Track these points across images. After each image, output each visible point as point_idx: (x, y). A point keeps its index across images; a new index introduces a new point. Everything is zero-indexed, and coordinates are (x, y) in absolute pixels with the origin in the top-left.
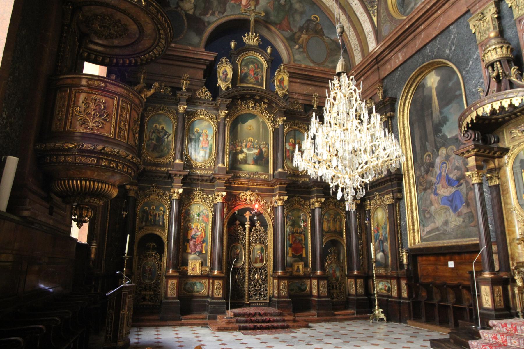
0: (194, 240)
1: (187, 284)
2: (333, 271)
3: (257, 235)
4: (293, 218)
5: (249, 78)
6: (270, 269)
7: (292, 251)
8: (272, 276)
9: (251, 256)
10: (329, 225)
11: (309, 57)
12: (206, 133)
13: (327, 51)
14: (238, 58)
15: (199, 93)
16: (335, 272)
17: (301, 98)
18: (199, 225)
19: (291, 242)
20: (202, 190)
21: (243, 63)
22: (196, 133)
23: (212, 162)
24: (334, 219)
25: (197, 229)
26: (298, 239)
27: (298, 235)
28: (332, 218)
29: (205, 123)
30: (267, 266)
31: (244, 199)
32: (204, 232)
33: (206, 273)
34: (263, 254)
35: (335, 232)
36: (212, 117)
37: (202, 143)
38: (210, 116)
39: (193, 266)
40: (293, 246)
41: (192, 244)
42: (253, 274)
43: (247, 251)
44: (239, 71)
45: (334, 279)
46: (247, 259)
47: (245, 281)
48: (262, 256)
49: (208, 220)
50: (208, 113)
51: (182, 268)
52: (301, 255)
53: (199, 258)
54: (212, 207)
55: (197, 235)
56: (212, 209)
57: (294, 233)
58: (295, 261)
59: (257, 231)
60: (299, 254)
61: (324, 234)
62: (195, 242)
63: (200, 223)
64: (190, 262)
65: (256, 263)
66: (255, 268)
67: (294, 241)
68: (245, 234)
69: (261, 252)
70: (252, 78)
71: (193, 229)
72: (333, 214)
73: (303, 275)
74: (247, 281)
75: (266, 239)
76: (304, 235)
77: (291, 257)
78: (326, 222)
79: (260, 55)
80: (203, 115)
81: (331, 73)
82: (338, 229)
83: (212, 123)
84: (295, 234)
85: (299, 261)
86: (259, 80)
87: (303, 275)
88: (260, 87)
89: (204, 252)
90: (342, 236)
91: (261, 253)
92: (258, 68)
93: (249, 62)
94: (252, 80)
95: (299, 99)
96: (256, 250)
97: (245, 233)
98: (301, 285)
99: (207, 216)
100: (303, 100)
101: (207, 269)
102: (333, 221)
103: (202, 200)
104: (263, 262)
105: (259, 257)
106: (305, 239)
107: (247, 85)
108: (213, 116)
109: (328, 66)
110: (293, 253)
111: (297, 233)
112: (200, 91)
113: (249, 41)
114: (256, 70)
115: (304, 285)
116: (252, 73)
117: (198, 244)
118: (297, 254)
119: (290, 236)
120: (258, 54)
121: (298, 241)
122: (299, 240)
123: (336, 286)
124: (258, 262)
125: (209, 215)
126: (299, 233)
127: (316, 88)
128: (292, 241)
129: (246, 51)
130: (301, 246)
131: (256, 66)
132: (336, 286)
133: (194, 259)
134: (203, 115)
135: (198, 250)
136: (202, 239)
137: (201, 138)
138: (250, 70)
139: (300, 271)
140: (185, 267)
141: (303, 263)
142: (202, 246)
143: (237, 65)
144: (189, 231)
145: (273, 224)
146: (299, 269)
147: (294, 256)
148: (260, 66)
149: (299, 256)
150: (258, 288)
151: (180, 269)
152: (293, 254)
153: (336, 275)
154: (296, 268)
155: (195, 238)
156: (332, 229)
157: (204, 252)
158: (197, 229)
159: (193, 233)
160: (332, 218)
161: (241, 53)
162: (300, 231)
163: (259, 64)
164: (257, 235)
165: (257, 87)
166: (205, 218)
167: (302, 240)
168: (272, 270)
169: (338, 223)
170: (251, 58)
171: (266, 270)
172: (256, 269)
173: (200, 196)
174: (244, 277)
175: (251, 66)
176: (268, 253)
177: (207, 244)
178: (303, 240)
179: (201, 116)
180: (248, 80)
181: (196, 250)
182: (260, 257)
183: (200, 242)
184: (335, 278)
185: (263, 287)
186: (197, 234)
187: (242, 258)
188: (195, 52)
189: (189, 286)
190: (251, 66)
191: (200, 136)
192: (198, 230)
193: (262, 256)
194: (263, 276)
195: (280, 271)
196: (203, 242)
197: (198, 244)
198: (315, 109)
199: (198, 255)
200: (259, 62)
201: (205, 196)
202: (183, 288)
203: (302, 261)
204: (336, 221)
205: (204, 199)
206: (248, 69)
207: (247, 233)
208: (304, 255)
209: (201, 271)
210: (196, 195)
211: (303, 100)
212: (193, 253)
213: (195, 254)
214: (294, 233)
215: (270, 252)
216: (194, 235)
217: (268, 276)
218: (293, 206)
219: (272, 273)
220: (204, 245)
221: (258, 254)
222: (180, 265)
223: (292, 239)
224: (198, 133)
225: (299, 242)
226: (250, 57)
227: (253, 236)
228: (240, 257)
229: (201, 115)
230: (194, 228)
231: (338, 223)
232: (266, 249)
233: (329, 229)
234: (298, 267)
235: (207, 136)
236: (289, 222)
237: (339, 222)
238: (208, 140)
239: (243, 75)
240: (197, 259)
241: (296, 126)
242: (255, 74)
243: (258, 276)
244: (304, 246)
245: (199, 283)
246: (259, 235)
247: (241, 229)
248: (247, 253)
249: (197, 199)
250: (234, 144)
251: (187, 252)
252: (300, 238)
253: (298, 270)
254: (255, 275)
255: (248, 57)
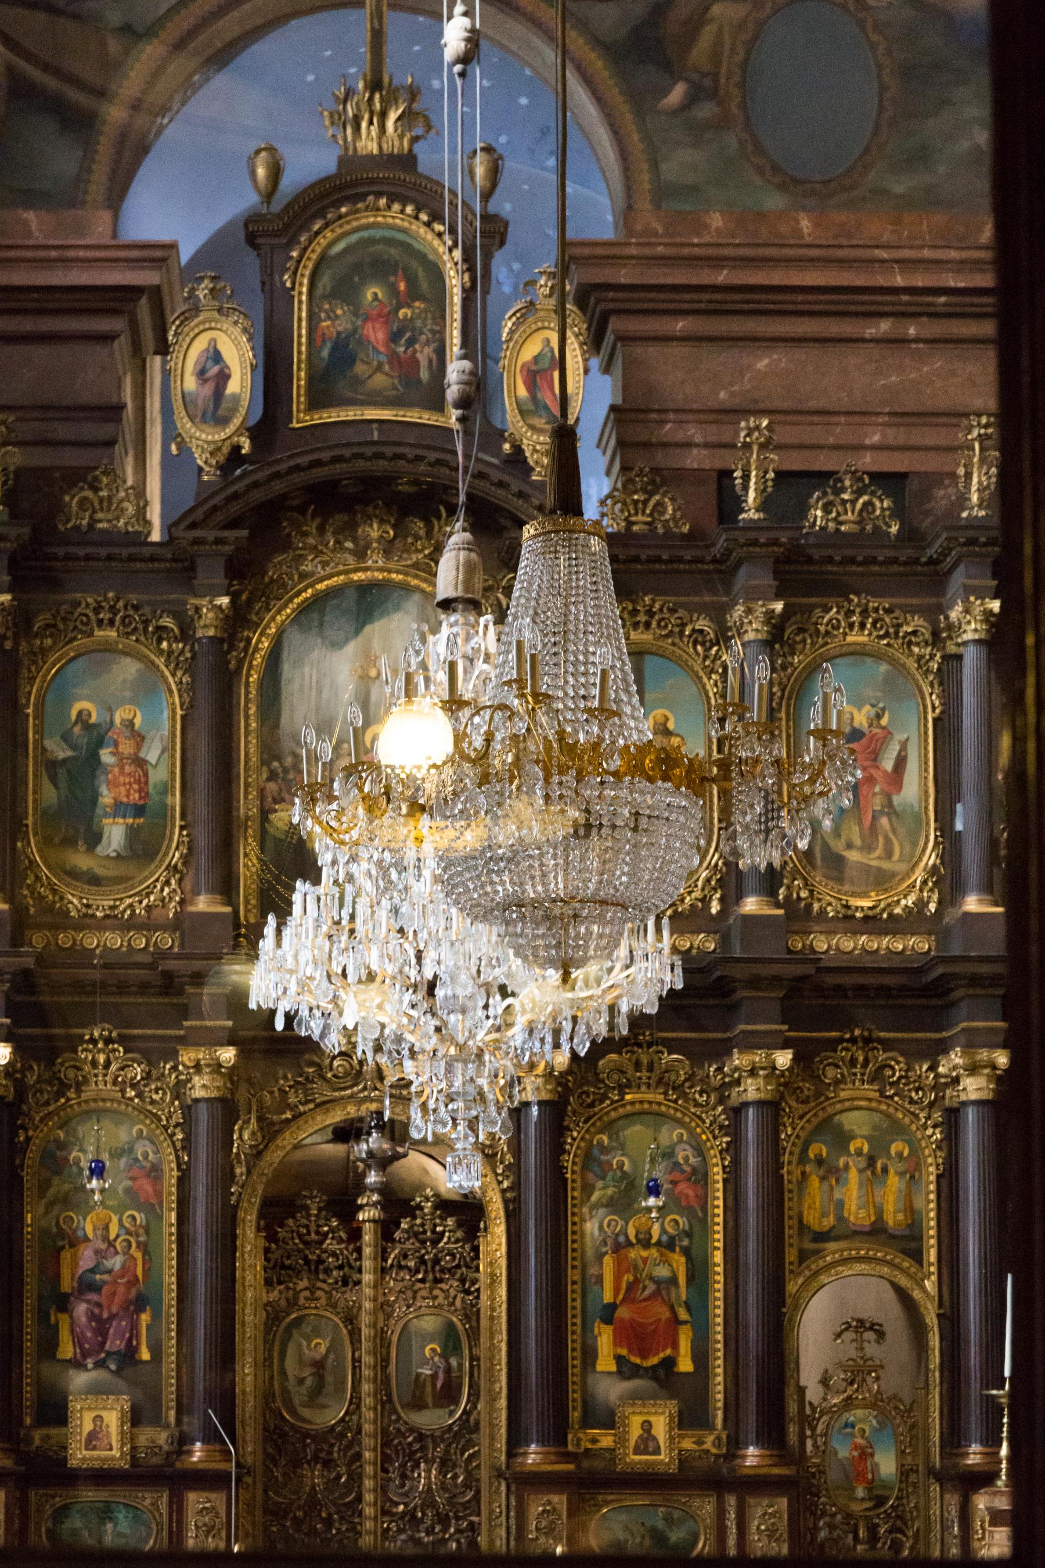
0: (93, 1297)
1: (62, 1513)
2: (856, 1447)
3: (422, 1261)
4: (621, 1165)
5: (360, 368)
6: (492, 1438)
7: (617, 1341)
8: (500, 1475)
9: (392, 1368)
10: (837, 1195)
11: (759, 149)
12: (131, 723)
13: (883, 88)
14: (295, 254)
15: (83, 503)
16: (865, 1454)
17: (698, 439)
18: (115, 1219)
19: (608, 1297)
20: (122, 1040)
21: (325, 281)
22: (77, 730)
23: (167, 883)
24: (871, 1161)
25: (105, 1238)
26: (651, 1278)
27: (654, 1253)
28: (859, 1153)
29: (128, 669)
30: (477, 1423)
31: (347, 1074)
32: (138, 1255)
33: (155, 1460)
34: (454, 1362)
35: (877, 1231)
36: (159, 628)
37: (113, 784)
38: (146, 623)
39: (88, 1426)
40: (623, 1313)
41: (84, 1319)
42: (403, 1466)
43: (365, 1345)
44: (301, 331)
45: (860, 1492)
46: (366, 1387)
47: (359, 1499)
48: (448, 1370)
49: (159, 1194)
50: (136, 608)
51: (37, 1436)
52: (669, 1363)
53: (120, 1383)
54: (177, 1125)
55: (109, 1272)
56: (180, 1136)
57: (630, 1244)
58: (635, 1397)
59: (423, 1242)
60: (654, 1361)
61: (809, 1245)
62: (99, 1305)
63: (120, 1210)
64: (75, 1405)
65: (418, 1405)
66: (412, 1430)
67: (631, 1287)
68: (360, 1258)
69: (444, 1347)
70: (379, 368)
71: (87, 1239)
72: (865, 1131)
73: (673, 1469)
74: (369, 1497)
75: (474, 1281)
76: (686, 1252)
77: (610, 1373)
78: (823, 1179)
79: (424, 217)
80: (111, 622)
81: (884, 254)
82: (894, 1217)
83: (160, 662)
84: (634, 1254)
85: (655, 1397)
86: (424, 375)
87: (673, 1469)
88: (427, 418)
89: (145, 1355)
90: (917, 1255)
91: (445, 1356)
92: (414, 294)
93: (357, 268)
94: (380, 381)
95: (689, 445)
96: (415, 1344)
97: (359, 1250)
98: (668, 1519)
99: (155, 1172)
100: (706, 445)
101: (162, 1437)
102: (861, 1171)
103: (123, 1091)
104: (456, 1402)
105: (434, 1377)
106: (690, 1279)
107: (350, 414)
108: (167, 622)
109: (886, 192)
110: (624, 1352)
111: (646, 1243)
112: (88, 493)
113: (357, 129)
114: (402, 313)
115: (682, 1521)
116: (376, 334)
117: (112, 1317)
118: (644, 1357)
119: (608, 1260)
120: (409, 209)
121: (651, 1287)
122: (658, 1282)
123: (873, 1529)
124: (429, 1400)
125: (166, 1168)
126: (659, 1243)
127: (800, 354)
128: (617, 1290)
129: (338, 203)
130: (665, 1314)
131: (402, 286)
132: (873, 1529)
133: (96, 1390)
134: (111, 622)
135: (115, 1343)
136: (133, 1292)
137: (106, 756)
138: (367, 318)
139: (657, 1451)
140: (53, 1431)
141: (672, 1406)
142: (134, 1327)
143: (288, 296)
144: (66, 1255)
145: (506, 1202)
146: (655, 1439)
147: (625, 1370)
148: (424, 286)
149: (653, 1367)
150: (428, 1534)
151: (29, 1440)
152: (619, 1359)
153: (876, 1466)
154: (635, 1432)
155: (95, 1288)
156: (857, 1214)
157: (145, 1355)
158: (105, 1238)
159: (86, 1259)
160: (859, 1153)
161: (313, 217)
162: (663, 1231)
163: (421, 273)
164: (422, 1261)
165: (413, 416)
166: (146, 1185)
167: (673, 1281)
168: (502, 1444)
169: (894, 1182)
170: (372, 241)
171: (470, 1444)
172: (421, 1437)
173: (114, 1067)
174: (356, 1478)
175: (372, 292)
176: (482, 1352)
177: (156, 1316)
178: (682, 1280)
179: (99, 633)
180: (357, 382)
181: (103, 1343)
182: (441, 1375)
183: (126, 1306)
184: (870, 1489)
185: (458, 1531)
186: (108, 1264)
187: (344, 1382)
188: (53, 254)
189: (78, 1524)
190: (372, 292)
191: (100, 743)
192: (111, 1244)
193: (448, 1370)
194: (455, 1477)
195: (533, 1447)
196: (140, 1303)
197: (112, 1317)
198: (753, 515)
199: (117, 1373)
200: (422, 257)
201: (138, 1071)
202: (48, 1531)
203: (671, 1398)
204: (885, 1170)
205: (133, 1086)
206: (355, 314)
207: (367, 1251)
208: (685, 1365)
209: (134, 1448)
210: (94, 1063)
211: (706, 445)
212: (90, 1363)
213: (100, 1364)
214: (630, 1244)
215: (493, 1348)
216: (92, 1271)
217: (484, 1474)
218: (622, 1095)
219: (503, 1458)
220: (145, 1318)
221: (425, 1362)
222: (28, 1421)
223: (617, 1280)
224: (88, 727)
225: (656, 1294)
226: (365, 234)
227: (400, 1267)
228: (329, 1379)
229: (100, 622)
230: (90, 1234)
231: (894, 1182)
232: (474, 1334)
233: (840, 1218)
234: (647, 1426)
235: (139, 738)
236: (600, 1184)
237: (901, 1174)
238: (140, 763)
239: (325, 353)
240: (109, 1392)
241: (648, 625)
242: (395, 337)
243: (428, 1471)
244: (683, 1315)
245: (126, 1505)
246: (436, 1261)
247: (332, 1230)
248: (367, 1359)
249: (100, 1086)
250: (286, 771)
251: (60, 1355)
252: (662, 1272)
253: (647, 1443)
254: (417, 1466)
255: (353, 238)
